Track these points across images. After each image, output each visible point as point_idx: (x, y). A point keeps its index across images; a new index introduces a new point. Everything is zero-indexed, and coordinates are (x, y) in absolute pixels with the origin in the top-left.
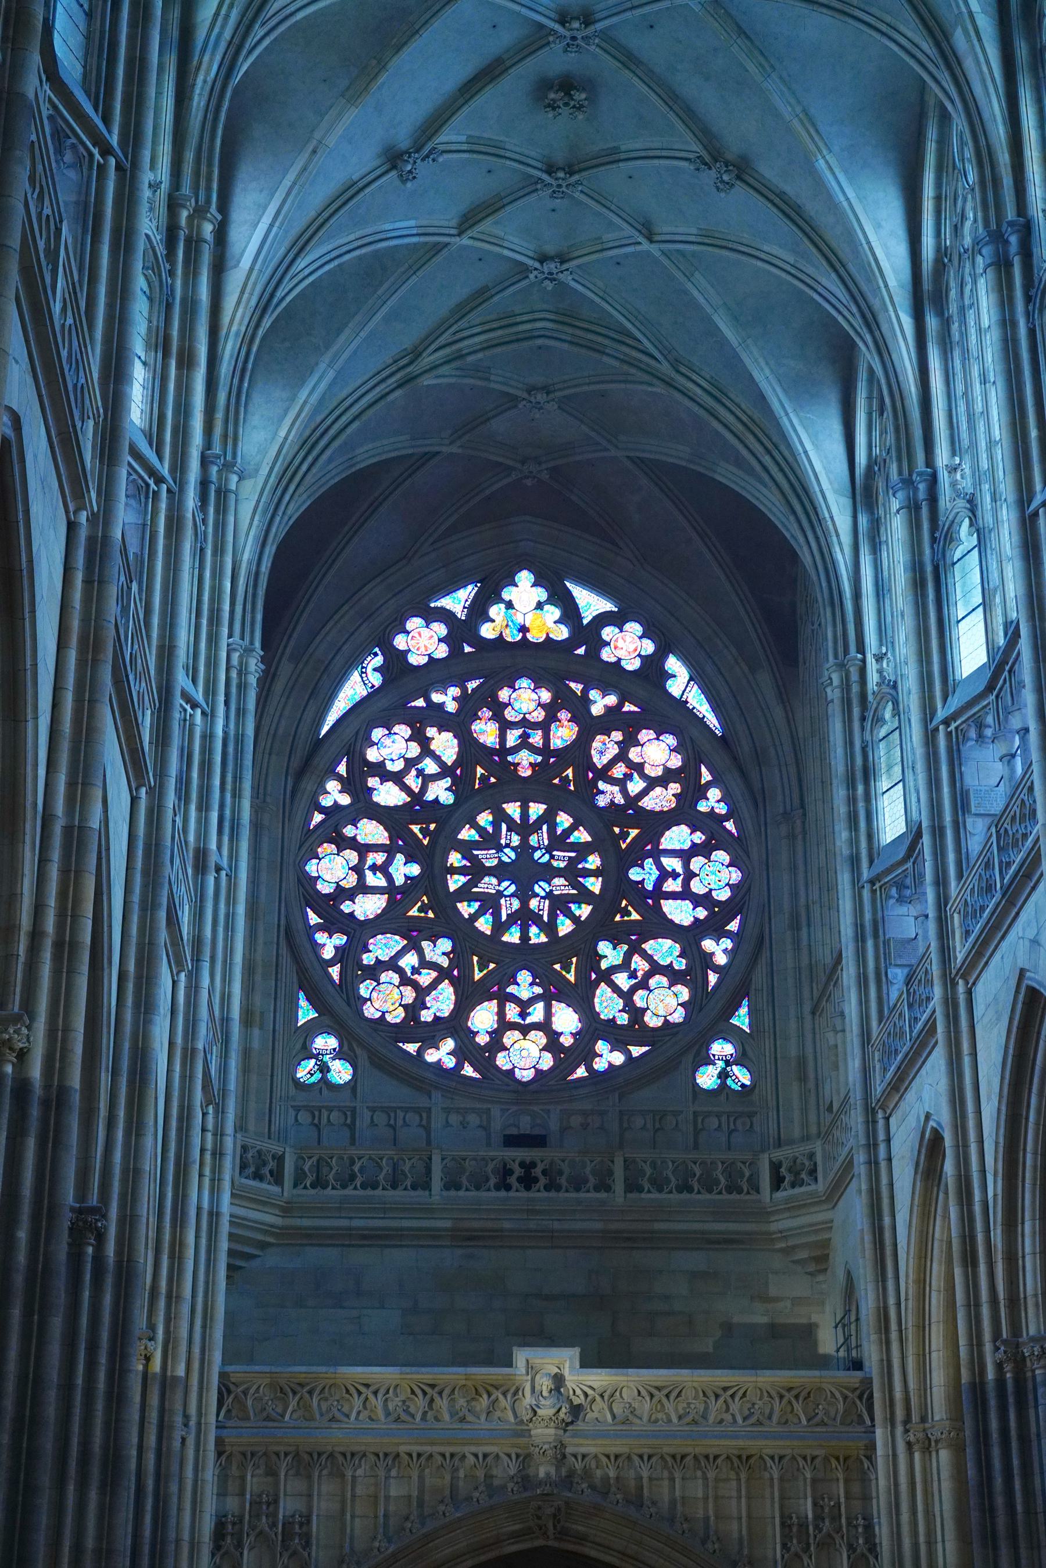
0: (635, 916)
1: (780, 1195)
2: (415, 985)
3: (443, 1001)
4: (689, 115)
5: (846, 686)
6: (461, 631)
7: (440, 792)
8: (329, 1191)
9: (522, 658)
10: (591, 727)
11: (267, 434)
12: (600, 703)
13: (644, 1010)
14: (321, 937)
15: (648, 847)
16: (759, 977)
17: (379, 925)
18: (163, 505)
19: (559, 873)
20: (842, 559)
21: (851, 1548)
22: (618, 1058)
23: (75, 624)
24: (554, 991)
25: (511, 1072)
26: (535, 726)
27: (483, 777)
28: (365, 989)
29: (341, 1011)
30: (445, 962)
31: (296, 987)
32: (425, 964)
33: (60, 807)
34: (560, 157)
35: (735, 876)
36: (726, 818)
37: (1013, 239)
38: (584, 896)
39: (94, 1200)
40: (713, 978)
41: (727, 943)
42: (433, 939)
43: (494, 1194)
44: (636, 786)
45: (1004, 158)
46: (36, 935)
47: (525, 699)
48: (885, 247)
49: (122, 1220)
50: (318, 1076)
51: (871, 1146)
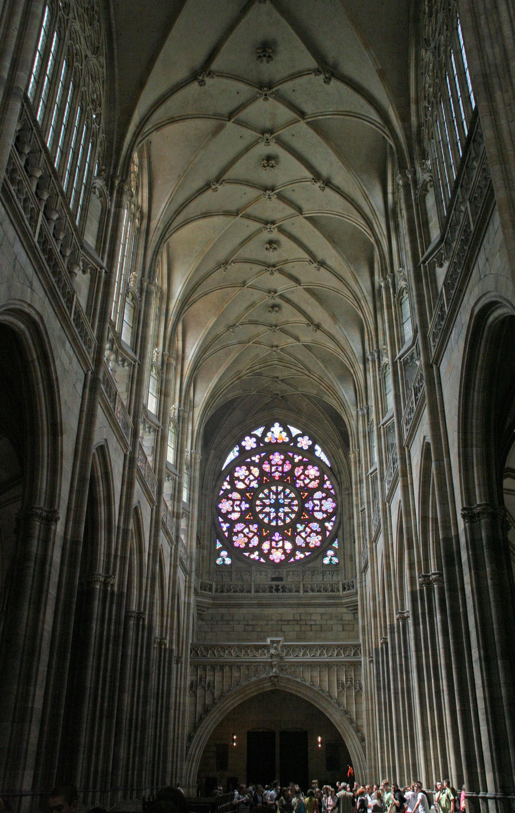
0: (307, 517)
1: (344, 593)
2: (248, 537)
4: (303, 313)
5: (355, 458)
6: (259, 440)
7: (254, 484)
8: (224, 594)
10: (294, 466)
11: (201, 397)
12: (297, 459)
13: (309, 543)
14: (223, 525)
15: (310, 498)
16: (340, 533)
17: (238, 521)
18: (160, 433)
19: (286, 505)
20: (353, 423)
21: (355, 688)
22: (302, 556)
23: (126, 479)
24: (285, 538)
25: (274, 560)
26: (280, 465)
29: (228, 545)
30: (256, 531)
33: (122, 525)
34: (274, 323)
35: (334, 505)
36: (331, 489)
37: (376, 355)
38: (293, 512)
39: (142, 610)
40: (328, 533)
41: (332, 524)
42: (253, 524)
43: (268, 594)
44: (307, 481)
45: (373, 333)
46: (116, 556)
47: (277, 458)
48: (355, 347)
49: (149, 615)
50: (222, 562)
51: (361, 582)
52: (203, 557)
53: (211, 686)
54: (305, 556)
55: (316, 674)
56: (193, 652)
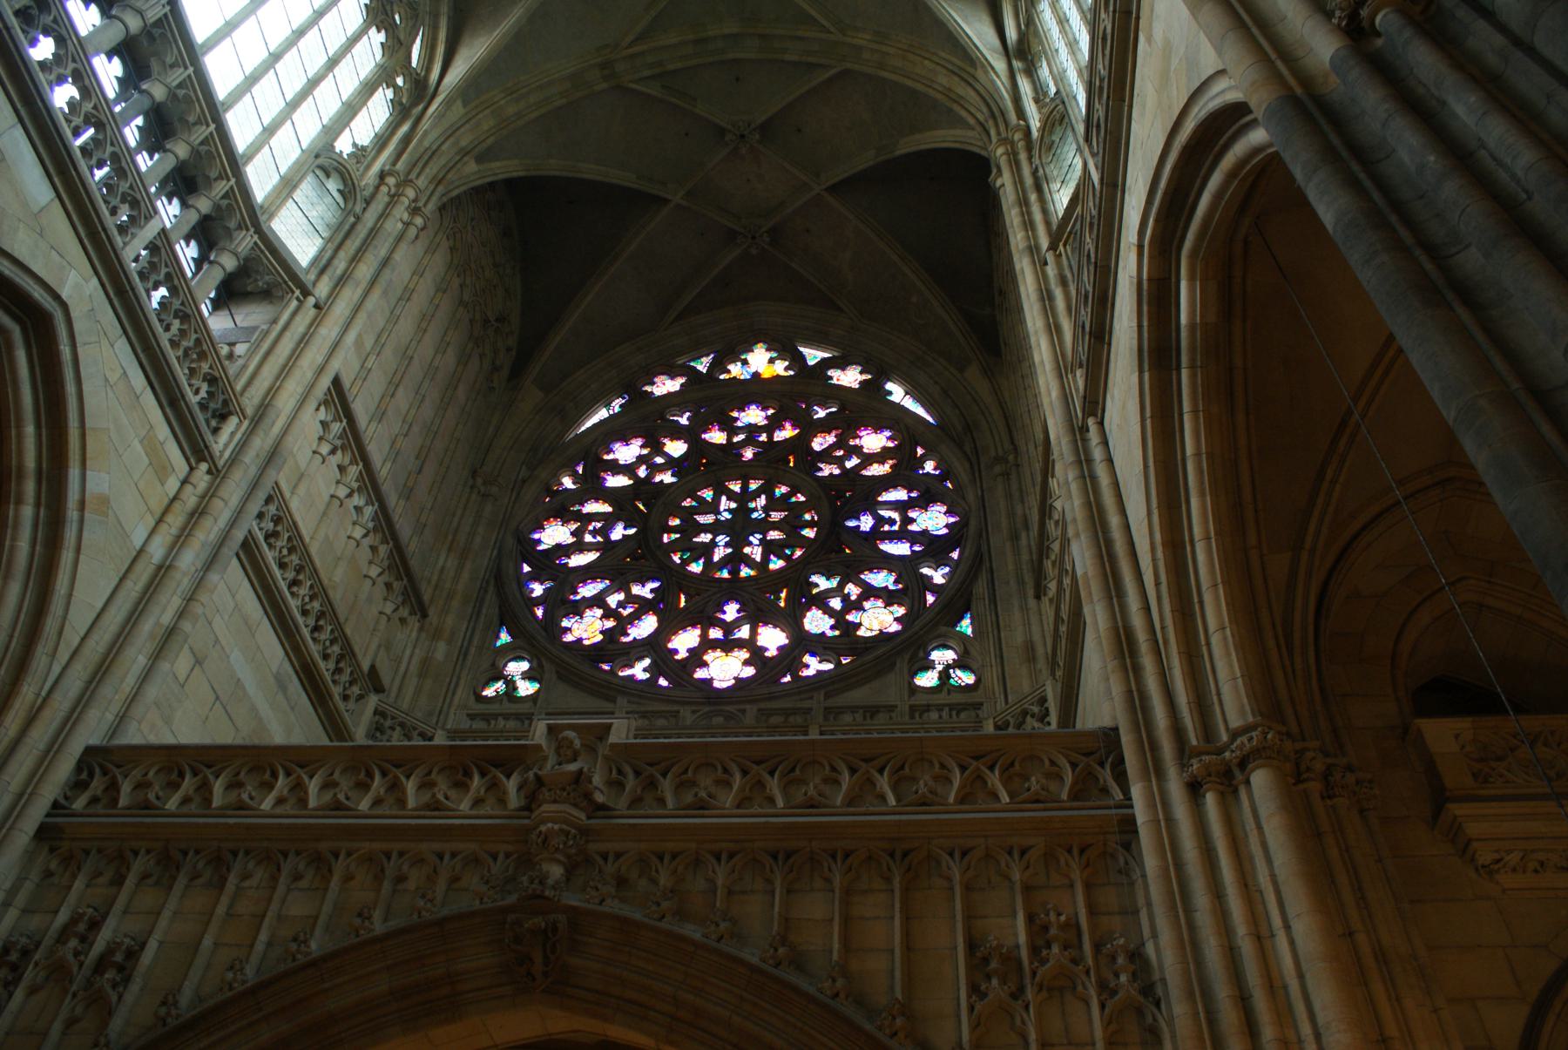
3: (646, 626)
9: (756, 390)
16: (980, 587)
27: (706, 466)
31: (496, 620)
32: (631, 599)
40: (930, 599)
52: (426, 663)
54: (838, 664)
55: (816, 907)
56: (97, 785)
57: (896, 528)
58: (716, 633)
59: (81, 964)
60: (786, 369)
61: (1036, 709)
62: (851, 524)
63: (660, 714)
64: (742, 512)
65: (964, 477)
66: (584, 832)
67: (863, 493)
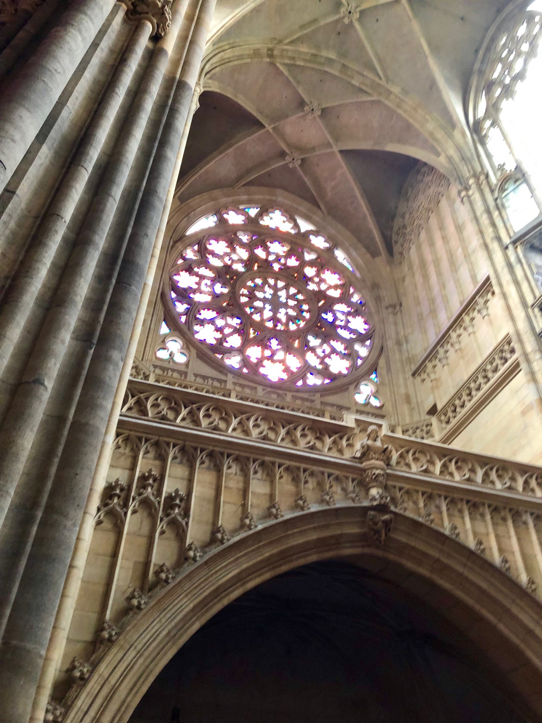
16: (382, 362)
17: (207, 306)
24: (288, 349)
28: (196, 328)
31: (162, 318)
32: (227, 325)
53: (179, 503)
57: (342, 324)
58: (268, 353)
59: (159, 503)
60: (292, 228)
61: (424, 428)
62: (324, 315)
63: (248, 387)
64: (275, 295)
65: (373, 309)
66: (388, 475)
67: (330, 302)
